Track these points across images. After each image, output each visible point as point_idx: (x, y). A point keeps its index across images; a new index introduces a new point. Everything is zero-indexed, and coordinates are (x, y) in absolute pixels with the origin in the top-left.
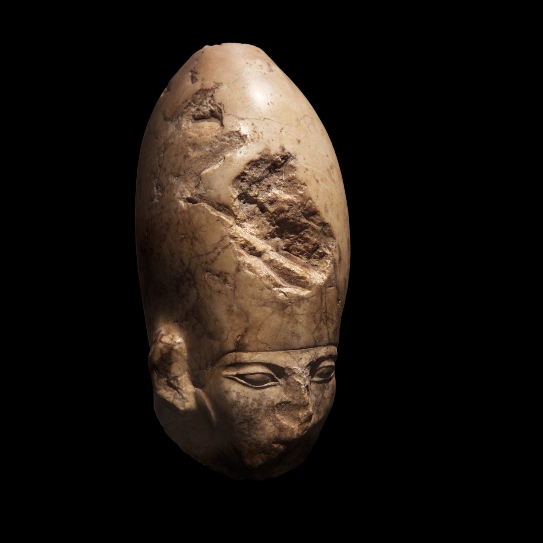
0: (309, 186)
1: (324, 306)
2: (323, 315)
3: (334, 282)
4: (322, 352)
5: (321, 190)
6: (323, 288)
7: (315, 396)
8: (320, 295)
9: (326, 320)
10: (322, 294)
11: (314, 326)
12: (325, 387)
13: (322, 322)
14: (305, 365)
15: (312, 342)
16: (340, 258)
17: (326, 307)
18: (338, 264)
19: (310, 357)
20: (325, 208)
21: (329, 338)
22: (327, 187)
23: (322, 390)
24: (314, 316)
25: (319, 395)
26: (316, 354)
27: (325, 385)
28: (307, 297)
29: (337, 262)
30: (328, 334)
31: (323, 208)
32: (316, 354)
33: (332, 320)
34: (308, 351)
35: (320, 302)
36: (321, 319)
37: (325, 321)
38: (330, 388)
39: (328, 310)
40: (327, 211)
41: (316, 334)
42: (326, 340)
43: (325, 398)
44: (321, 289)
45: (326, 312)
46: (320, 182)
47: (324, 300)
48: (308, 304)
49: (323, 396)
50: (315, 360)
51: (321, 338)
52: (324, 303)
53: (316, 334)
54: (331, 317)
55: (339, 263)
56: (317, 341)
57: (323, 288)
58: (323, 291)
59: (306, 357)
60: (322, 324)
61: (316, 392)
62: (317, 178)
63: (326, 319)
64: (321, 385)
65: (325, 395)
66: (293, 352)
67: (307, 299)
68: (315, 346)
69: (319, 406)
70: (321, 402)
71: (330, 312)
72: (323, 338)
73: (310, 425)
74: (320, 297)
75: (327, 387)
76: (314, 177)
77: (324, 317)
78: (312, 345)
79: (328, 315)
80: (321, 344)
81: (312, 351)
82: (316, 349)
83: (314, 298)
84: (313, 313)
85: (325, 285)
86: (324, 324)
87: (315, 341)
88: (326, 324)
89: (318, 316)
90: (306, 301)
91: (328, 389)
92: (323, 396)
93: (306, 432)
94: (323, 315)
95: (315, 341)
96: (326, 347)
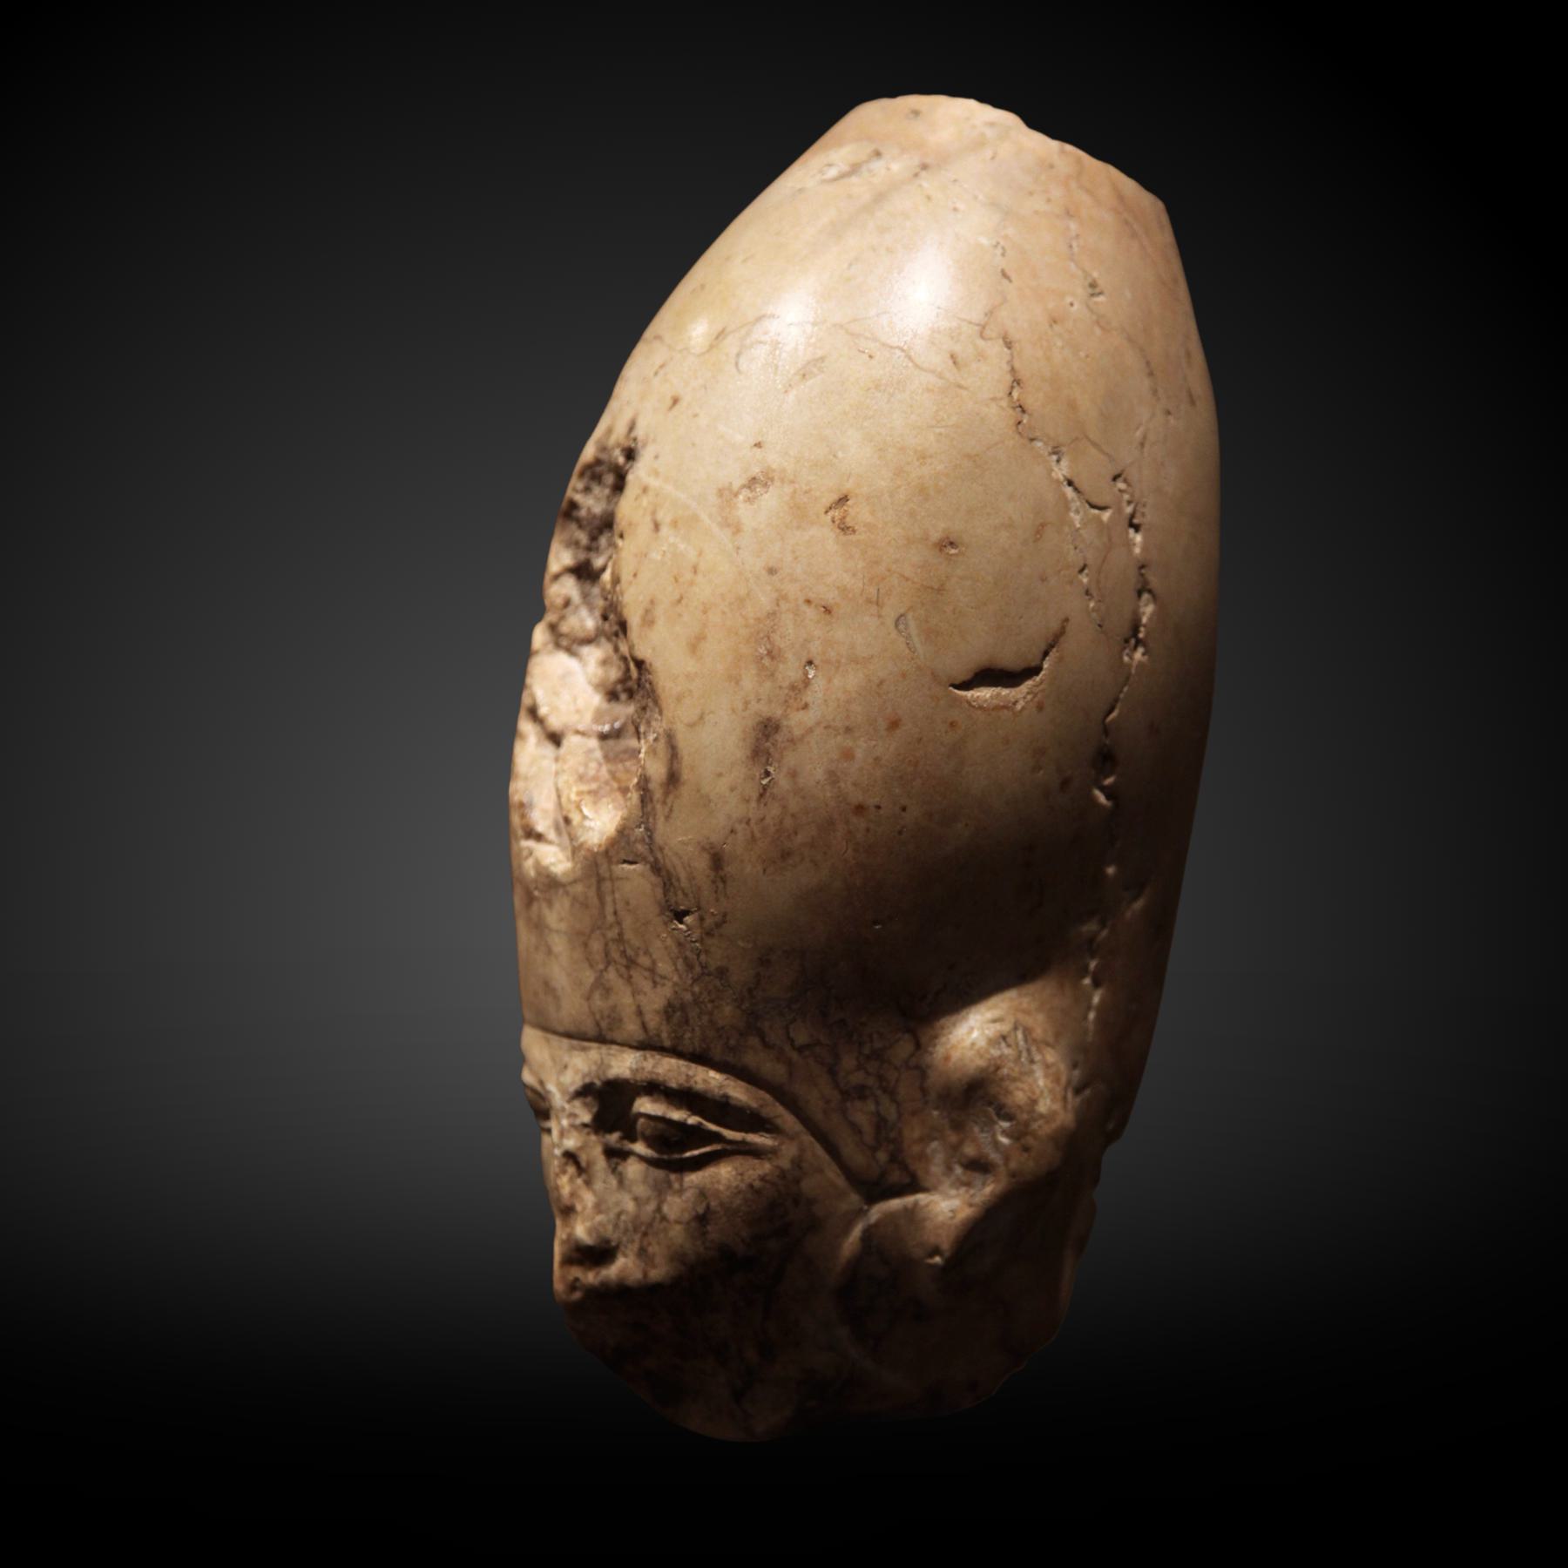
0: (627, 541)
1: (610, 918)
2: (613, 947)
3: (640, 848)
4: (624, 1064)
5: (656, 556)
6: (600, 860)
7: (636, 1199)
8: (594, 880)
9: (628, 967)
10: (600, 880)
11: (589, 977)
12: (669, 1185)
13: (611, 969)
14: (572, 1089)
15: (589, 1027)
16: (673, 779)
17: (619, 923)
18: (658, 795)
19: (586, 1069)
20: (647, 611)
21: (644, 1026)
22: (682, 547)
23: (661, 1190)
24: (586, 945)
25: (648, 1199)
26: (603, 1065)
27: (673, 1177)
28: (564, 880)
29: (655, 786)
30: (640, 1013)
31: (640, 612)
32: (603, 1065)
33: (652, 970)
34: (584, 1049)
35: (596, 901)
36: (609, 961)
37: (623, 970)
38: (689, 1194)
39: (628, 935)
40: (648, 621)
41: (598, 1002)
42: (632, 1028)
43: (664, 1218)
44: (596, 864)
45: (620, 939)
46: (664, 530)
47: (609, 899)
48: (566, 902)
49: (659, 1209)
50: (598, 1083)
51: (615, 1020)
52: (609, 909)
53: (598, 1002)
54: (644, 960)
55: (667, 793)
56: (604, 1024)
57: (600, 860)
58: (603, 870)
59: (580, 1065)
60: (611, 975)
61: (641, 1190)
62: (660, 516)
63: (624, 962)
64: (659, 1174)
65: (665, 1208)
66: (555, 1039)
67: (563, 885)
68: (601, 1039)
69: (645, 1234)
70: (650, 1225)
71: (636, 942)
72: (621, 1020)
73: (590, 1277)
74: (594, 889)
75: (676, 1186)
76: (654, 513)
77: (615, 955)
78: (561, 1029)
79: (630, 952)
80: (618, 1036)
81: (595, 1052)
82: (604, 1049)
83: (579, 888)
84: (579, 933)
85: (607, 852)
86: (621, 976)
87: (598, 1024)
88: (629, 979)
89: (596, 945)
90: (561, 891)
91: (681, 1192)
92: (659, 1209)
93: (577, 1295)
94: (613, 947)
95: (598, 1024)
96: (638, 1054)
